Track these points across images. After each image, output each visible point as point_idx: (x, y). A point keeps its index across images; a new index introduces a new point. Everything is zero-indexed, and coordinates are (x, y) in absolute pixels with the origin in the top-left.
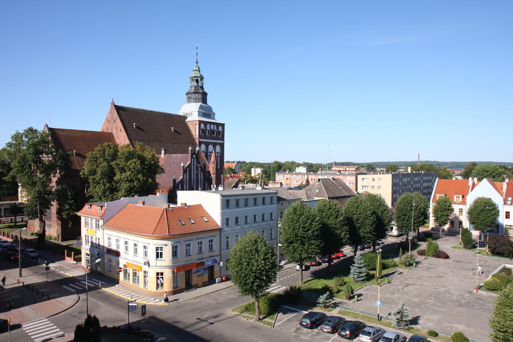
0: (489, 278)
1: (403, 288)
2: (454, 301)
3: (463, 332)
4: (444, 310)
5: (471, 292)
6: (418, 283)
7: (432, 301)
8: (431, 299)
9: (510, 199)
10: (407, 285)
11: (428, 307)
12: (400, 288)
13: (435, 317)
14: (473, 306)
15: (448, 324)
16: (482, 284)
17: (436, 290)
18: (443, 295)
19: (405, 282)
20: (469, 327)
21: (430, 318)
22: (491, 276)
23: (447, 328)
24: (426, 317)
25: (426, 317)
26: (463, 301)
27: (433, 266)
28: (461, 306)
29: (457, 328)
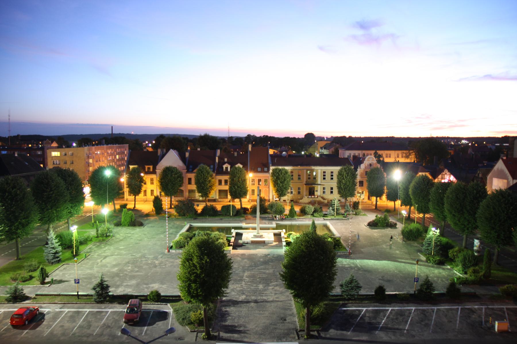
0: (178, 238)
1: (101, 261)
2: (149, 264)
3: (158, 290)
4: (141, 274)
5: (164, 254)
6: (116, 254)
7: (130, 268)
8: (129, 266)
9: (191, 167)
10: (105, 257)
11: (126, 274)
12: (99, 261)
13: (134, 282)
14: (165, 265)
15: (145, 286)
16: (171, 245)
17: (133, 257)
18: (140, 260)
19: (104, 254)
20: (162, 283)
21: (129, 284)
22: (178, 235)
23: (144, 289)
24: (125, 284)
25: (125, 284)
26: (156, 262)
27: (129, 235)
28: (155, 266)
29: (153, 287)
